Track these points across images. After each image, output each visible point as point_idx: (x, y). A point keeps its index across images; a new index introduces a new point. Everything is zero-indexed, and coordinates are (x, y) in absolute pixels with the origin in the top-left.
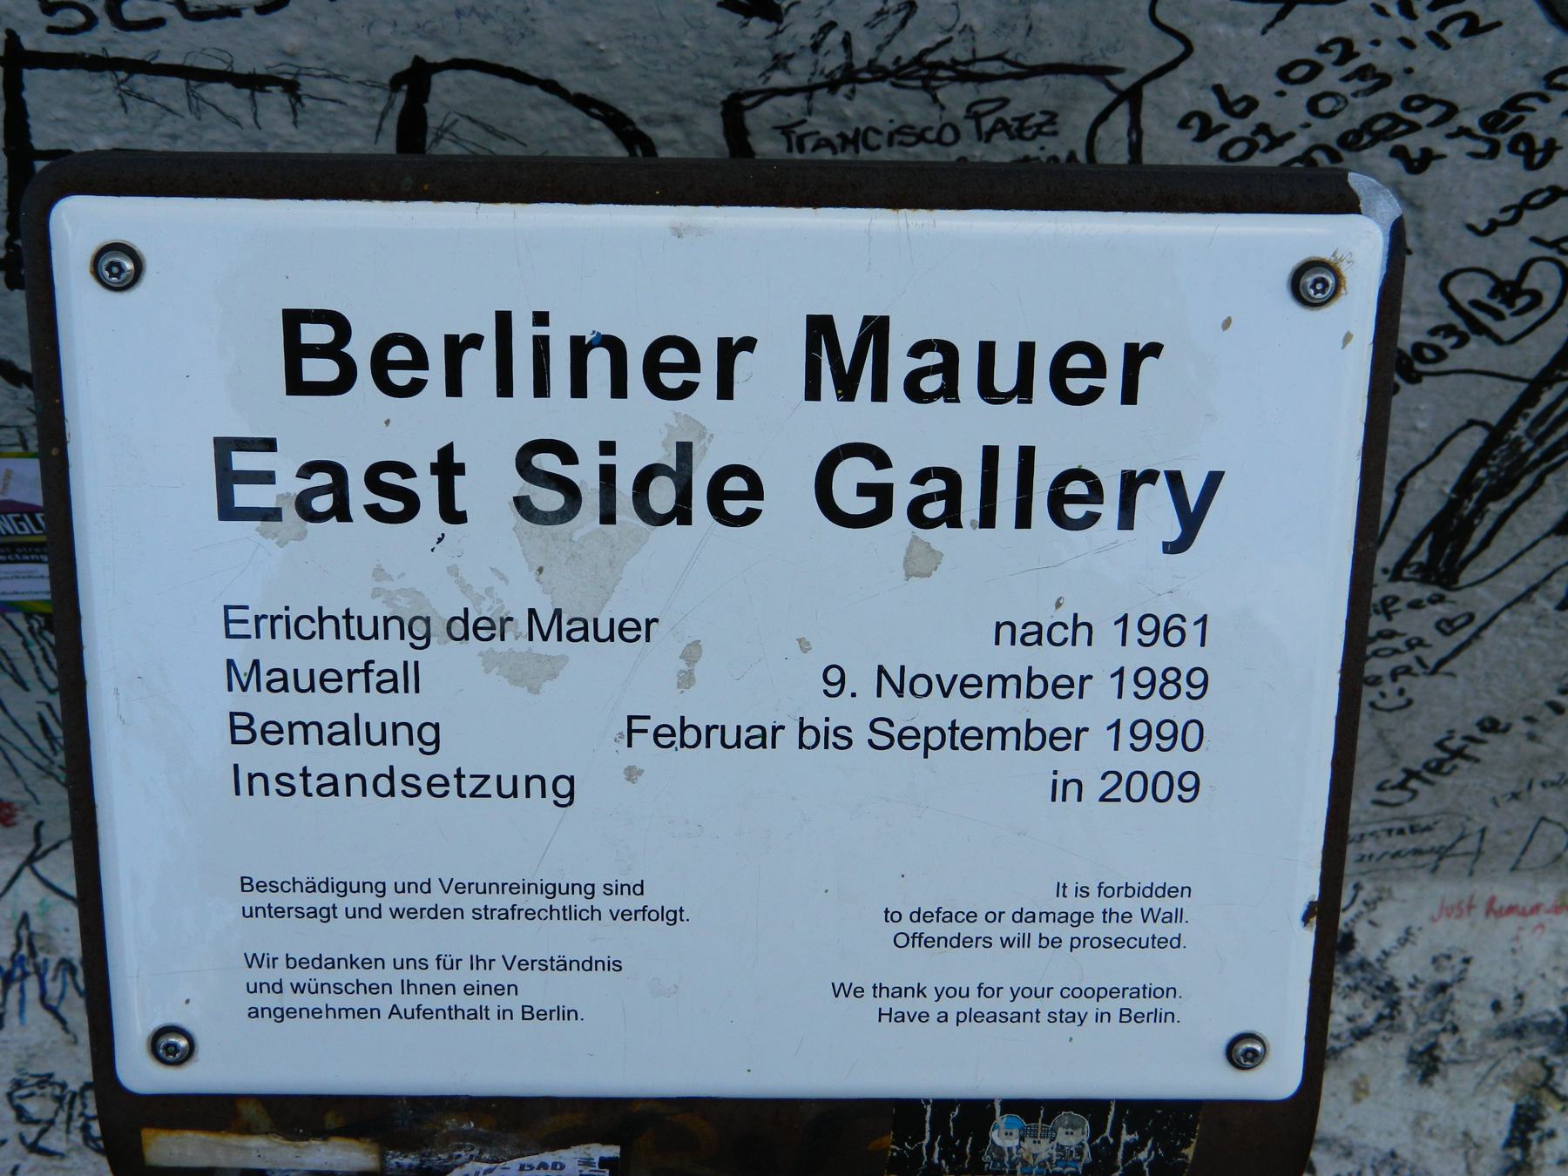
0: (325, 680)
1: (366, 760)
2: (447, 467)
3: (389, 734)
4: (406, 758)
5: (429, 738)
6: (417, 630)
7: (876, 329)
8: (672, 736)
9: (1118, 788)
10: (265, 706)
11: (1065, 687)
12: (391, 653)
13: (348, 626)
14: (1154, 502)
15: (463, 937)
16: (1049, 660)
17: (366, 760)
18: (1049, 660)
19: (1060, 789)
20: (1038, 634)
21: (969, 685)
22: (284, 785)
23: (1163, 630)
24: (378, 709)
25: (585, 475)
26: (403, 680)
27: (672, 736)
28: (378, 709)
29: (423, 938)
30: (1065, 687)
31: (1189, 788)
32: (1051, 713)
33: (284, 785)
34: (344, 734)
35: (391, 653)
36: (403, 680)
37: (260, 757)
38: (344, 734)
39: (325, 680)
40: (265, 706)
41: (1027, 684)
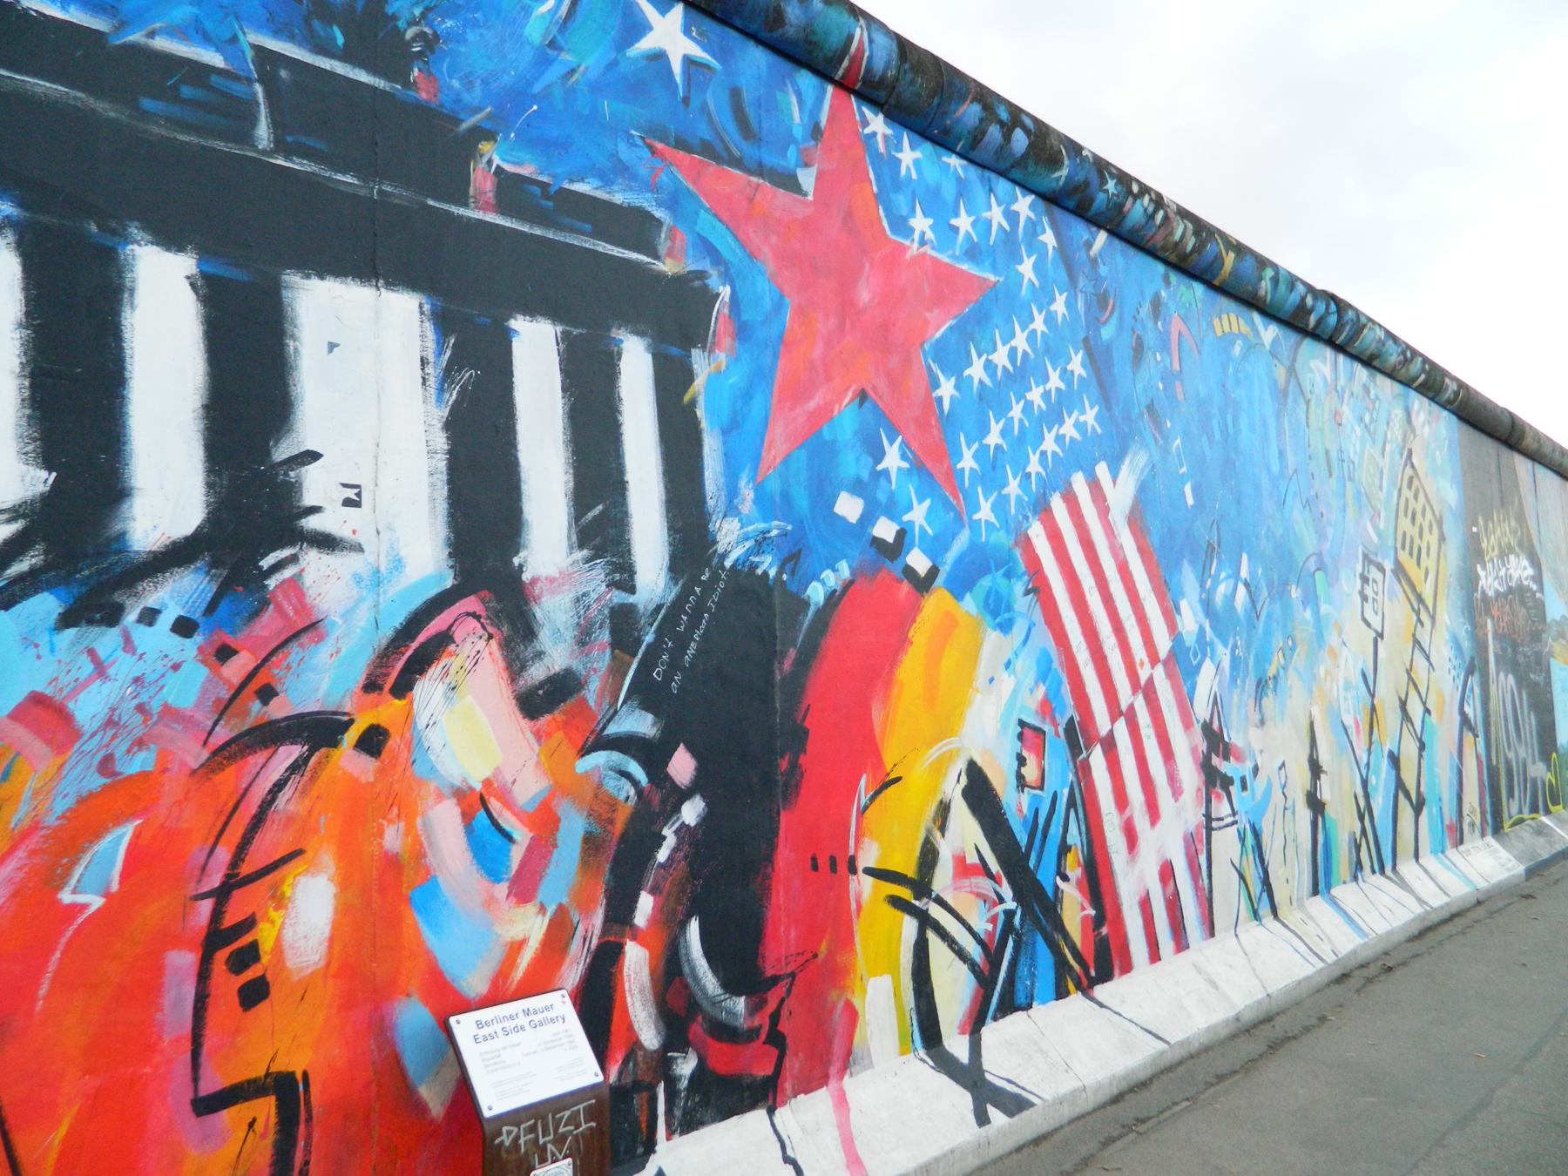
0: (492, 1058)
5: (504, 1062)
6: (498, 1050)
8: (527, 1054)
10: (487, 1063)
11: (560, 1039)
12: (497, 1053)
13: (492, 1052)
17: (498, 1066)
20: (554, 1035)
21: (553, 1041)
22: (492, 1071)
24: (499, 1059)
26: (499, 1056)
27: (527, 1054)
28: (499, 1059)
30: (560, 1039)
31: (576, 1047)
32: (561, 1042)
33: (492, 1071)
35: (497, 1053)
38: (496, 1064)
39: (492, 1058)
40: (487, 1063)
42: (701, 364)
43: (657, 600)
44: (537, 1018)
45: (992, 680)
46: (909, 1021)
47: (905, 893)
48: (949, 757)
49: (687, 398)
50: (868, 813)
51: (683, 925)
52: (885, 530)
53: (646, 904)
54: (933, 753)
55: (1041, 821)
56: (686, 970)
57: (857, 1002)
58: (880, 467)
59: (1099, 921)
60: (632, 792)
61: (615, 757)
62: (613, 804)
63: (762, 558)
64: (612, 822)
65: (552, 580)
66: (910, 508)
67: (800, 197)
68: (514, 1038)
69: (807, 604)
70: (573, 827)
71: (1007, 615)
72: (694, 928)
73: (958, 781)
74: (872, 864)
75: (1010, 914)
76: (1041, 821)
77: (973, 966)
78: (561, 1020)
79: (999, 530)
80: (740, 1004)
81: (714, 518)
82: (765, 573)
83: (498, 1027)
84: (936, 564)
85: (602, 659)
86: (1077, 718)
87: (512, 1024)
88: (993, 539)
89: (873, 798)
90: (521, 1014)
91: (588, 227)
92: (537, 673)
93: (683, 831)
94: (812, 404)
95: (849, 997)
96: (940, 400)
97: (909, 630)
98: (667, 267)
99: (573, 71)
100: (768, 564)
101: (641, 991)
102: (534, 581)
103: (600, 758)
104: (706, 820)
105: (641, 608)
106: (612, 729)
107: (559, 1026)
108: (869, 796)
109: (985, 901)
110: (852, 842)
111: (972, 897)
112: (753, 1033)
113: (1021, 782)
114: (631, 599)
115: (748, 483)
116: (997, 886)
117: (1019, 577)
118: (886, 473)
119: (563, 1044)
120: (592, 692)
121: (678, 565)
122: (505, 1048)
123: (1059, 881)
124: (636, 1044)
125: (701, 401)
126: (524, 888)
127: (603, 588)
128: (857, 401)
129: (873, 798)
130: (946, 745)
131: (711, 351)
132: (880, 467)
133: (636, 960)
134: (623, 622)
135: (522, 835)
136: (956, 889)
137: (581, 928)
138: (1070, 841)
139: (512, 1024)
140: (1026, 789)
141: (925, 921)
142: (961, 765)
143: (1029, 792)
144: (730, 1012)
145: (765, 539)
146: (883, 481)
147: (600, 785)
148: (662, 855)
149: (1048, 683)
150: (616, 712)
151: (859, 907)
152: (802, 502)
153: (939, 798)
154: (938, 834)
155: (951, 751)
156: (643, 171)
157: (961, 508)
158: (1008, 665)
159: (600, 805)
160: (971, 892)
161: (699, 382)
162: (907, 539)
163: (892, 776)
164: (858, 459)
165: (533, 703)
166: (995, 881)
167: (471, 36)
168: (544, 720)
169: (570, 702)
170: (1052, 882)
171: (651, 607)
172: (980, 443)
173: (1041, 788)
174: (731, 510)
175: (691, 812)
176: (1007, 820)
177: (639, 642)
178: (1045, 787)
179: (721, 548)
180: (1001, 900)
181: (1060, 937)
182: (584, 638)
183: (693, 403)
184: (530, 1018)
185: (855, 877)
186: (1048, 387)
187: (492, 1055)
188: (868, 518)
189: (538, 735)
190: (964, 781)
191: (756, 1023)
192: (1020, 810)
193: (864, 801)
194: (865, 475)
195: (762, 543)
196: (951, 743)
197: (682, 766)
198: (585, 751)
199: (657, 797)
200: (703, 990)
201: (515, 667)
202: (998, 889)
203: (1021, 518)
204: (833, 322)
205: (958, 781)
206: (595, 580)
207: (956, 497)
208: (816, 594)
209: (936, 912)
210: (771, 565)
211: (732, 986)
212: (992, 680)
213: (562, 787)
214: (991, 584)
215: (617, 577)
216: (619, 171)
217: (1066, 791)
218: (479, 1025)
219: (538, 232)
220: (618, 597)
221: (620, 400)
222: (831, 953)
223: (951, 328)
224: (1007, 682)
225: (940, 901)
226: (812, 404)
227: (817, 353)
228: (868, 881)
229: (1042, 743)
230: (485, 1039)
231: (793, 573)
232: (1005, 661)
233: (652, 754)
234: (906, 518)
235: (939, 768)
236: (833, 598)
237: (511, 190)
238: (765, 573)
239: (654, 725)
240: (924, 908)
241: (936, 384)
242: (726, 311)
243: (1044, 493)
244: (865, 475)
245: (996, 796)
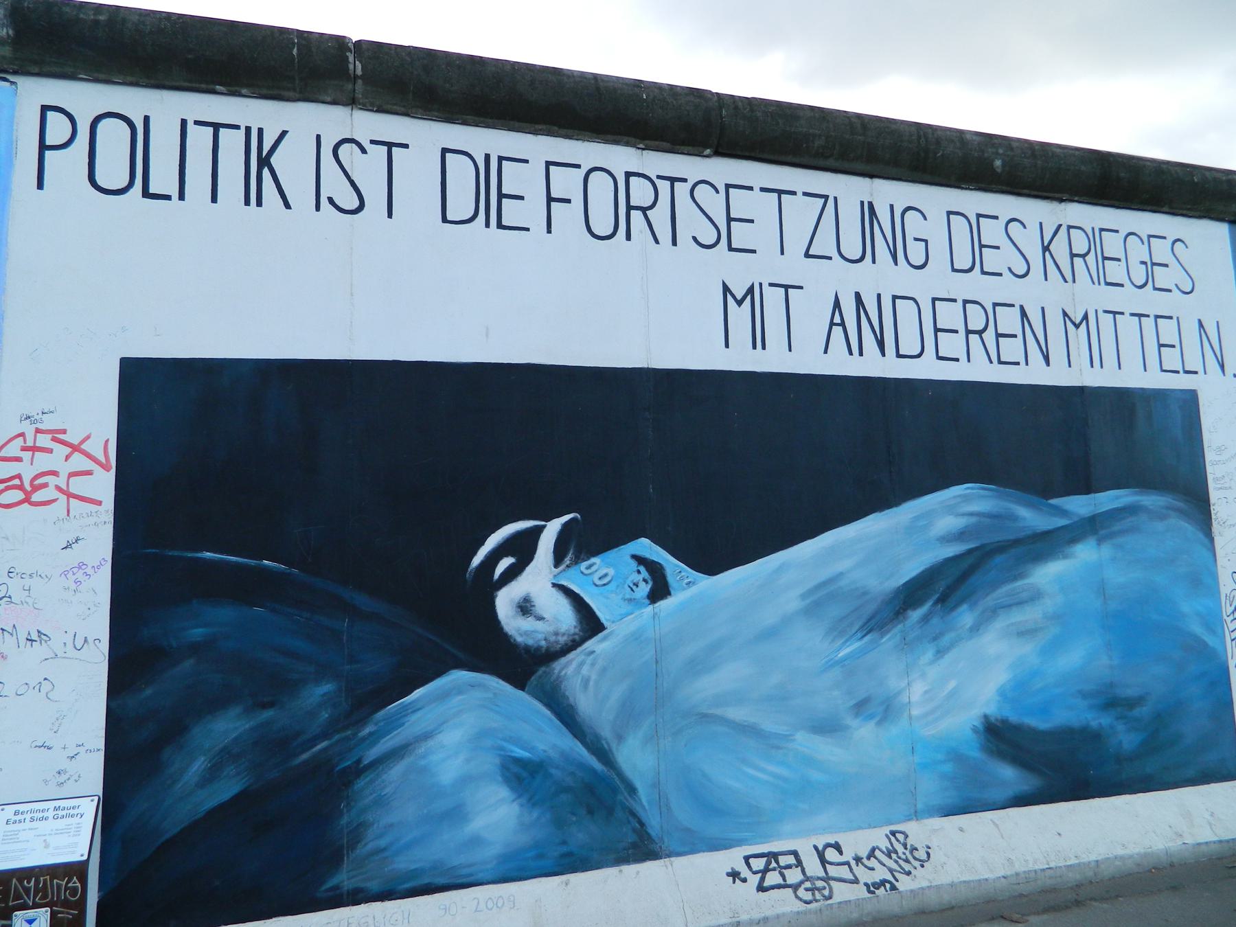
1: (12, 841)
2: (25, 819)
3: (14, 839)
4: (17, 840)
5: (18, 838)
6: (19, 831)
7: (59, 807)
9: (74, 835)
11: (70, 829)
13: (14, 831)
14: (79, 816)
15: (16, 854)
16: (70, 827)
18: (70, 827)
19: (69, 836)
20: (69, 825)
21: (62, 829)
23: (79, 824)
24: (14, 837)
25: (35, 819)
26: (17, 834)
28: (14, 837)
29: (12, 854)
34: (11, 839)
36: (17, 834)
37: (4, 842)
38: (11, 839)
41: (67, 829)
44: (60, 813)
68: (35, 824)
78: (79, 816)
83: (28, 816)
87: (41, 815)
90: (51, 810)
107: (76, 820)
119: (69, 832)
122: (24, 830)
139: (41, 815)
184: (56, 813)
187: (12, 833)
218: (16, 813)
230: (15, 822)
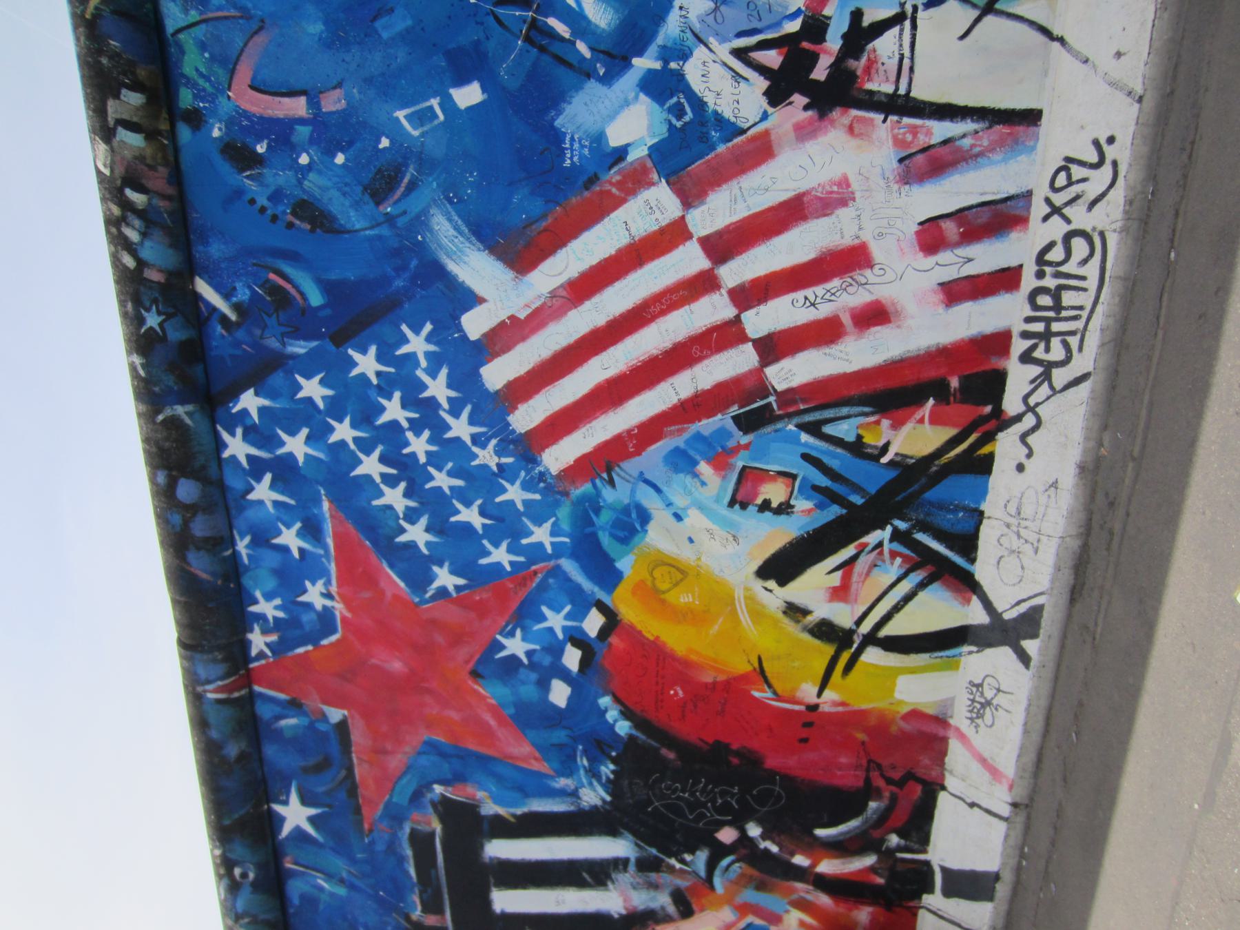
42: (490, 808)
43: (632, 846)
45: (691, 540)
46: (939, 660)
47: (845, 656)
48: (751, 599)
49: (512, 820)
50: (779, 691)
51: (816, 838)
52: (572, 658)
53: (800, 860)
54: (745, 618)
55: (823, 481)
56: (841, 838)
57: (904, 710)
58: (525, 661)
59: (939, 390)
60: (737, 865)
61: (717, 872)
62: (742, 875)
63: (603, 773)
64: (751, 877)
65: (625, 901)
66: (551, 630)
67: (350, 721)
69: (631, 738)
70: (750, 895)
71: (634, 515)
72: (820, 832)
73: (770, 591)
74: (815, 690)
75: (897, 536)
76: (823, 481)
77: (922, 585)
79: (558, 519)
80: (873, 805)
81: (582, 806)
82: (613, 772)
84: (594, 602)
85: (664, 878)
86: (735, 410)
88: (565, 526)
89: (770, 686)
91: (433, 872)
92: (671, 909)
93: (764, 836)
94: (492, 722)
95: (899, 716)
96: (457, 588)
97: (648, 639)
98: (437, 827)
99: (350, 872)
100: (607, 769)
101: (843, 864)
102: (626, 908)
103: (718, 881)
104: (760, 822)
105: (637, 855)
106: (703, 873)
108: (767, 690)
109: (876, 566)
110: (797, 707)
111: (867, 582)
112: (894, 799)
113: (785, 509)
114: (633, 860)
115: (556, 781)
116: (867, 549)
117: (598, 494)
118: (529, 654)
120: (683, 883)
121: (613, 832)
123: (884, 460)
124: (872, 869)
125: (512, 810)
126: (776, 919)
127: (627, 875)
128: (480, 680)
129: (770, 686)
130: (740, 602)
131: (479, 801)
132: (525, 661)
133: (827, 867)
134: (646, 865)
135: (751, 919)
136: (856, 600)
137: (803, 894)
138: (851, 438)
140: (792, 502)
141: (871, 639)
142: (758, 585)
143: (796, 498)
144: (875, 812)
145: (590, 771)
146: (536, 658)
147: (731, 882)
148: (774, 849)
149: (698, 457)
150: (694, 872)
151: (843, 704)
152: (560, 736)
153: (780, 615)
154: (809, 618)
155: (746, 598)
156: (386, 836)
157: (544, 567)
158: (678, 517)
159: (742, 881)
160: (863, 582)
161: (501, 811)
162: (578, 636)
163: (756, 665)
164: (523, 683)
165: (686, 911)
166: (862, 551)
167: (361, 920)
168: (695, 907)
169: (687, 894)
170: (883, 471)
171: (637, 849)
172: (483, 537)
173: (793, 477)
174: (574, 794)
175: (754, 831)
176: (814, 530)
177: (656, 857)
178: (794, 471)
179: (599, 803)
180: (880, 545)
181: (937, 462)
182: (654, 886)
183: (514, 816)
185: (821, 705)
186: (405, 424)
188: (565, 675)
189: (702, 910)
190: (771, 584)
191: (887, 794)
192: (810, 511)
193: (770, 695)
194: (534, 676)
195: (594, 773)
196: (739, 594)
197: (727, 835)
198: (712, 888)
199: (743, 851)
200: (857, 827)
201: (668, 919)
202: (870, 547)
203: (542, 485)
204: (428, 699)
205: (770, 591)
206: (625, 878)
207: (535, 573)
208: (623, 728)
209: (866, 627)
210: (607, 768)
211: (858, 810)
212: (691, 540)
213: (728, 900)
214: (607, 533)
215: (621, 867)
216: (392, 847)
217: (805, 437)
219: (446, 897)
220: (632, 867)
221: (523, 860)
222: (867, 730)
223: (392, 566)
224: (695, 519)
225: (859, 622)
226: (492, 722)
227: (454, 715)
228: (829, 695)
229: (755, 471)
231: (612, 748)
232: (673, 519)
233: (718, 852)
234: (560, 636)
235: (757, 613)
236: (627, 714)
237: (432, 906)
238: (613, 772)
239: (702, 851)
240: (861, 638)
241: (443, 592)
242: (450, 789)
243: (513, 442)
244: (534, 676)
245: (791, 543)
